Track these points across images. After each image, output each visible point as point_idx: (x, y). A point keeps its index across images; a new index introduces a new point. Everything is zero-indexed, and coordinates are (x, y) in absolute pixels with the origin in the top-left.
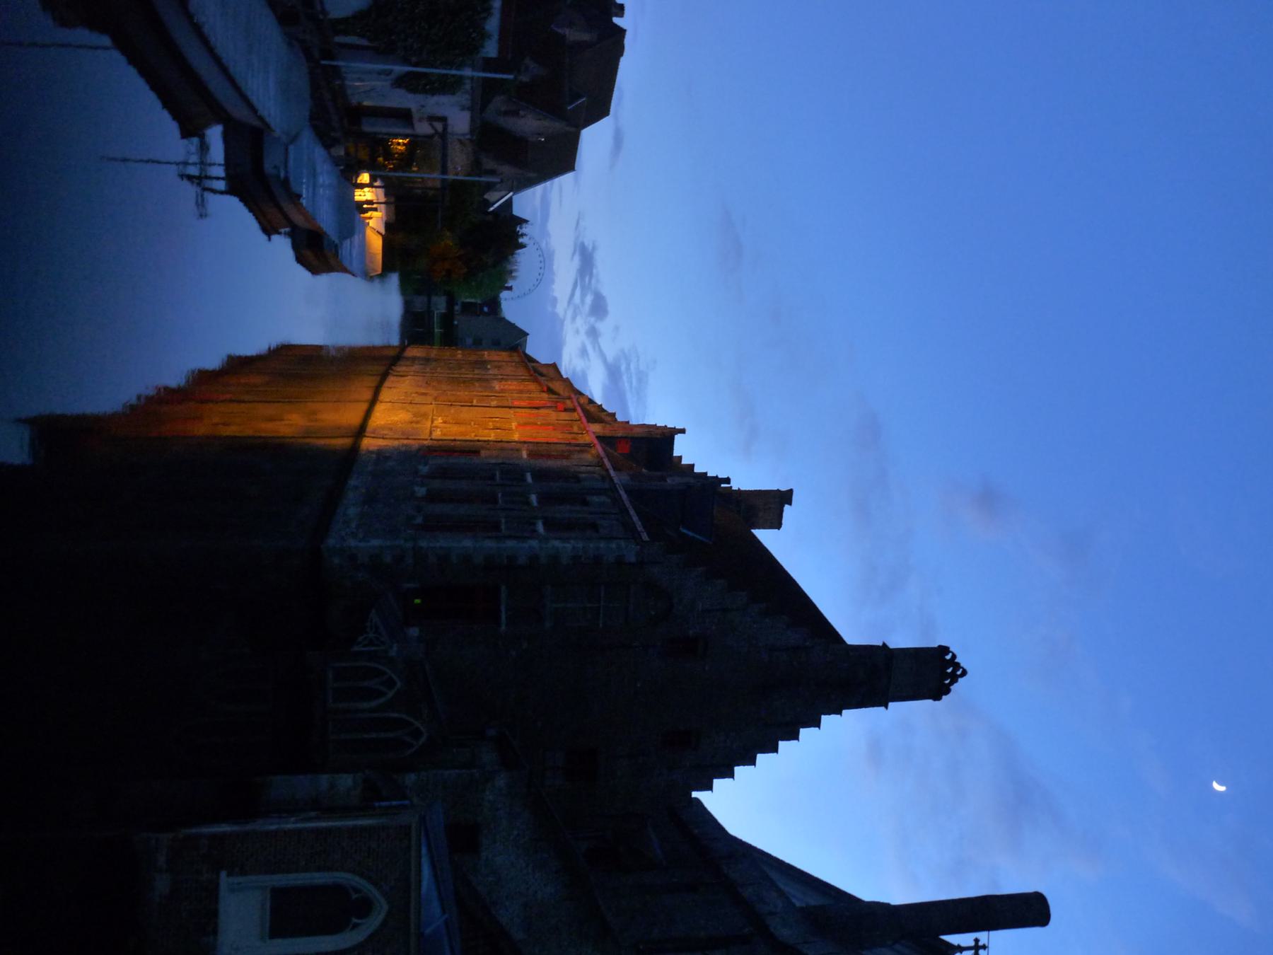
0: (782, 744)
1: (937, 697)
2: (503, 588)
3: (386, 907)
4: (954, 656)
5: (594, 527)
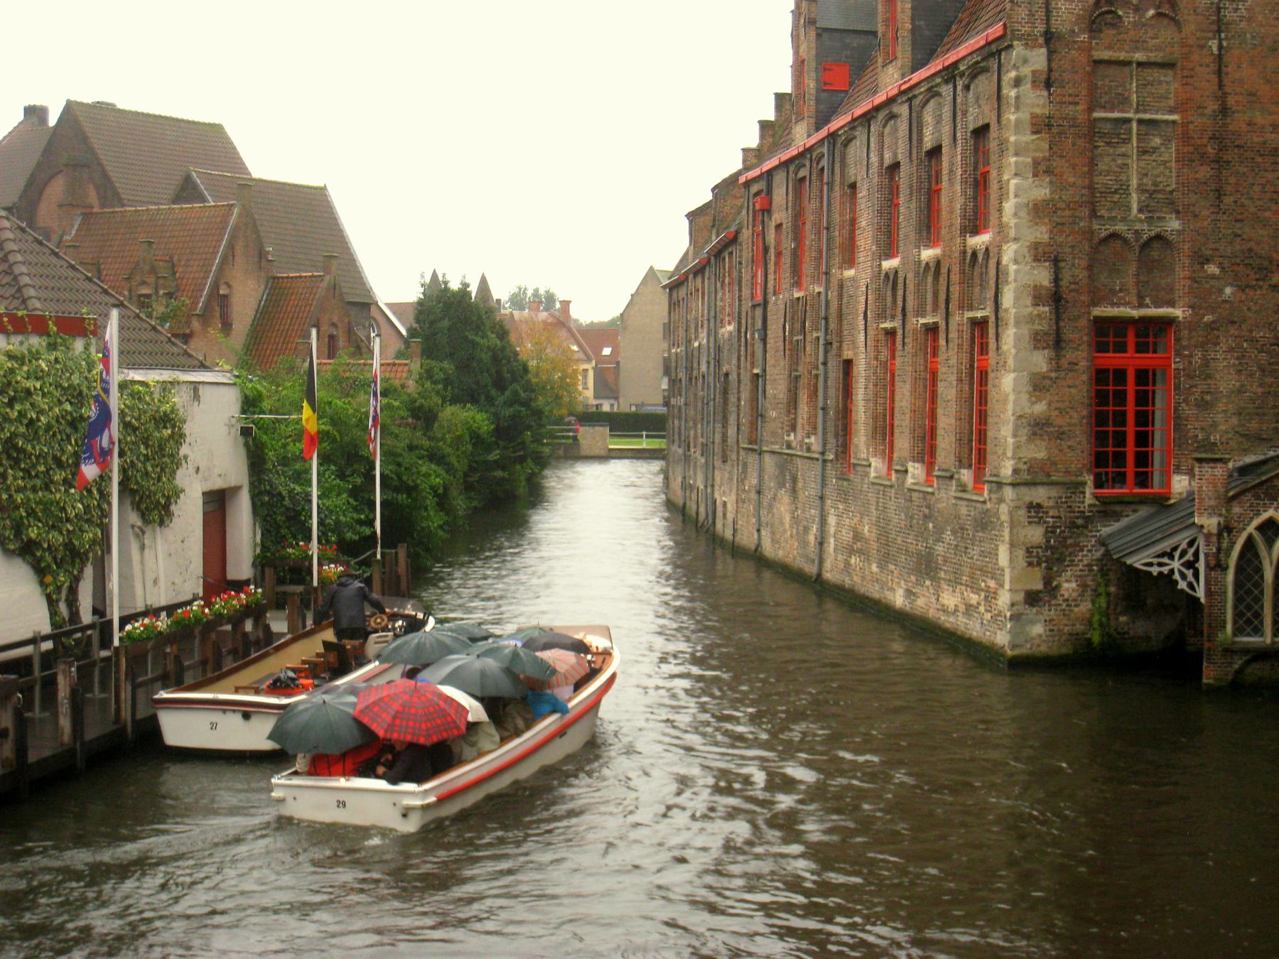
5: (981, 132)
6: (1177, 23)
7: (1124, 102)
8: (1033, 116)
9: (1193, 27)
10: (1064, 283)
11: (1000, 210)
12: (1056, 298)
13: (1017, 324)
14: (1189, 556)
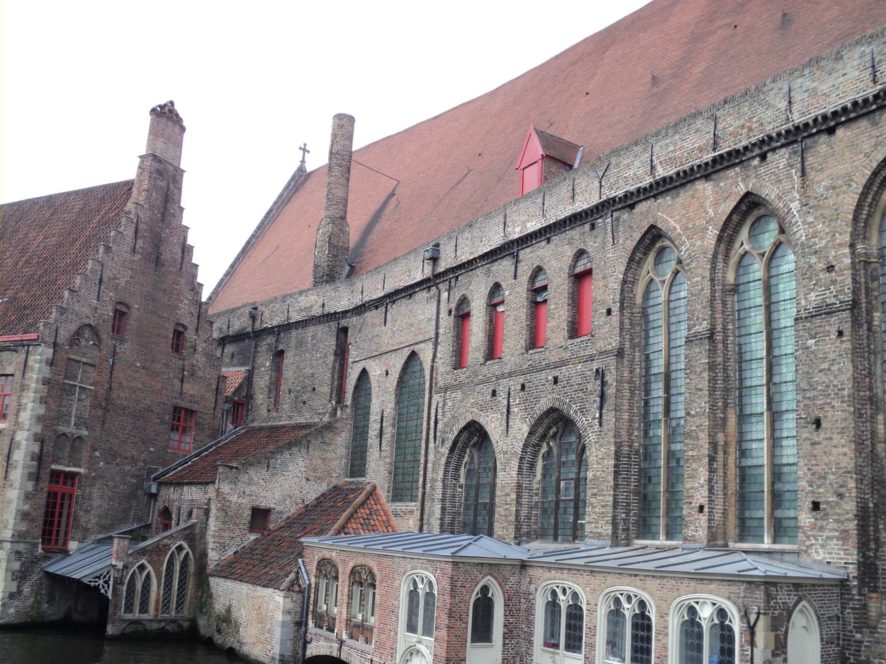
0: (193, 261)
1: (183, 129)
2: (53, 467)
3: (489, 577)
4: (160, 106)
6: (100, 349)
7: (75, 378)
8: (44, 377)
9: (105, 352)
10: (44, 452)
11: (17, 415)
12: (39, 459)
13: (24, 467)
14: (106, 579)
